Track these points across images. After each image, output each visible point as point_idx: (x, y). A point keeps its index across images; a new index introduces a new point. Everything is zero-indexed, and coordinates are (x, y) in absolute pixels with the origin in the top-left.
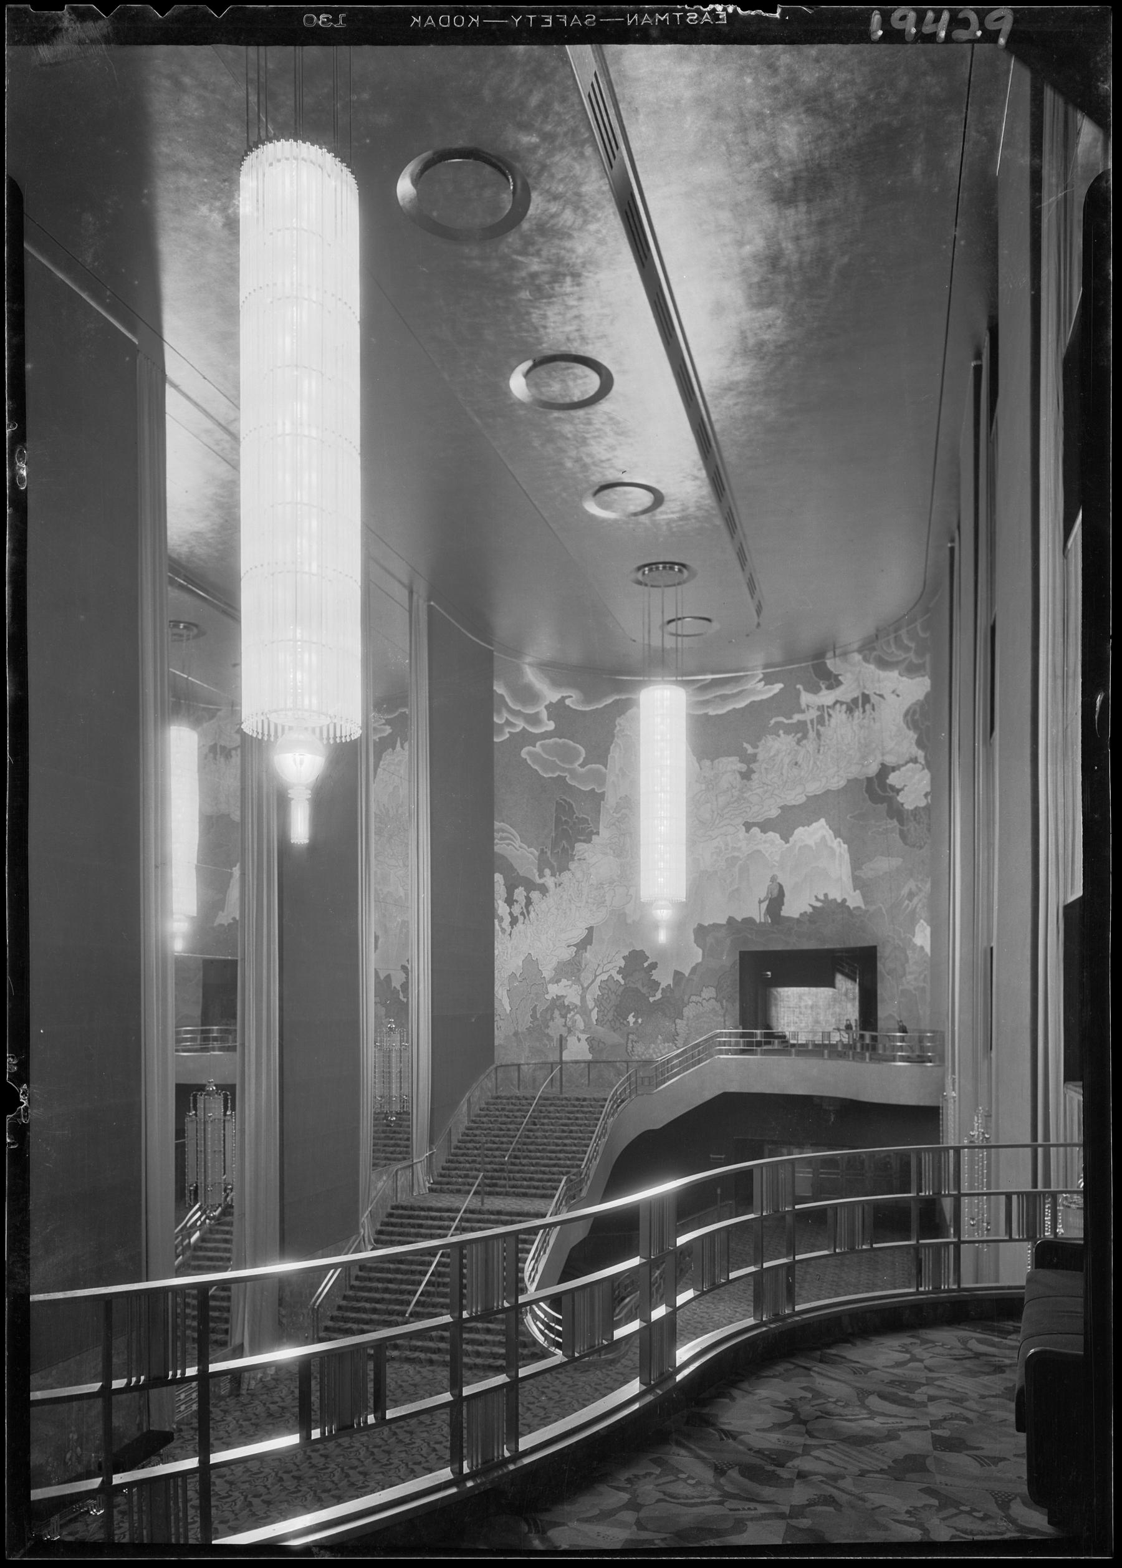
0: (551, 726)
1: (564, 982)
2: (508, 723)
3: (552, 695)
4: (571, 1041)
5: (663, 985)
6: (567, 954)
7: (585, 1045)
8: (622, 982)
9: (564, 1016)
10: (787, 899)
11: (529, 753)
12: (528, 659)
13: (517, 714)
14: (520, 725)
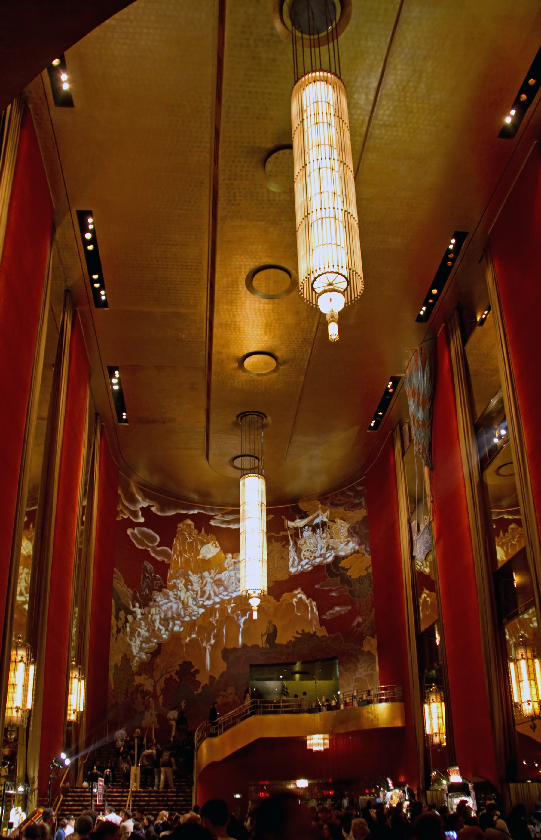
1: (144, 676)
4: (147, 714)
5: (203, 684)
7: (154, 718)
8: (178, 680)
9: (143, 698)
10: (278, 634)
13: (126, 508)
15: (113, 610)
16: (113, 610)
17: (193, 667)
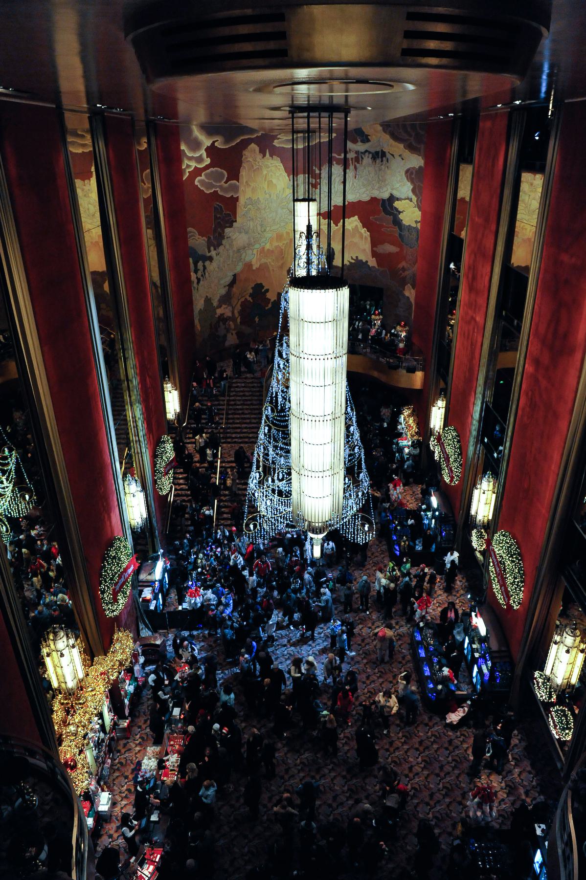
0: (208, 161)
1: (224, 306)
2: (188, 166)
3: (207, 142)
4: (229, 336)
5: (272, 300)
6: (223, 291)
7: (235, 336)
9: (224, 324)
11: (199, 181)
12: (195, 123)
13: (190, 159)
14: (193, 164)
17: (263, 287)
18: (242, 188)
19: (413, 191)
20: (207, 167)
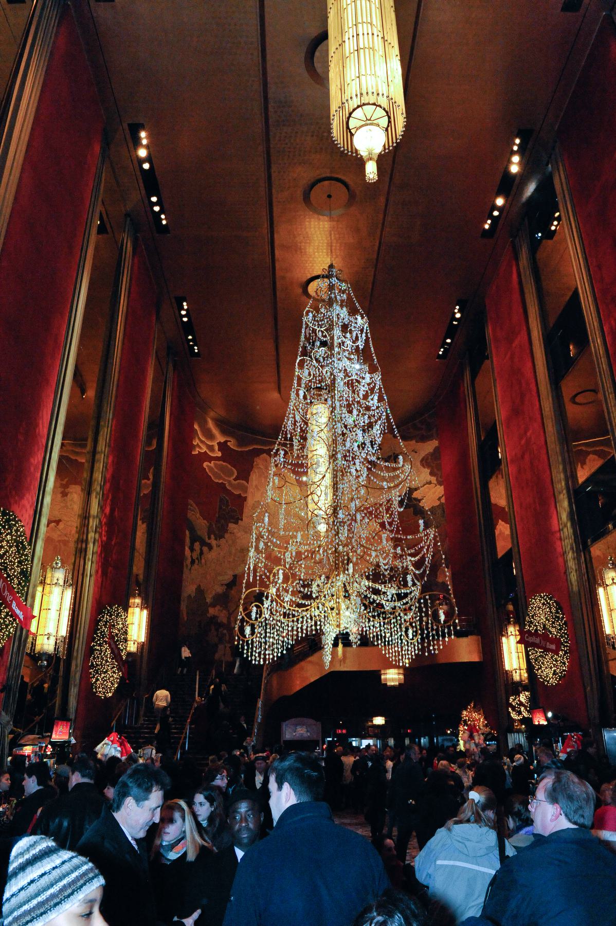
0: (219, 454)
1: (218, 607)
3: (221, 439)
6: (220, 590)
12: (212, 414)
15: (188, 540)
16: (188, 540)
18: (250, 490)
19: (431, 474)
20: (217, 459)
